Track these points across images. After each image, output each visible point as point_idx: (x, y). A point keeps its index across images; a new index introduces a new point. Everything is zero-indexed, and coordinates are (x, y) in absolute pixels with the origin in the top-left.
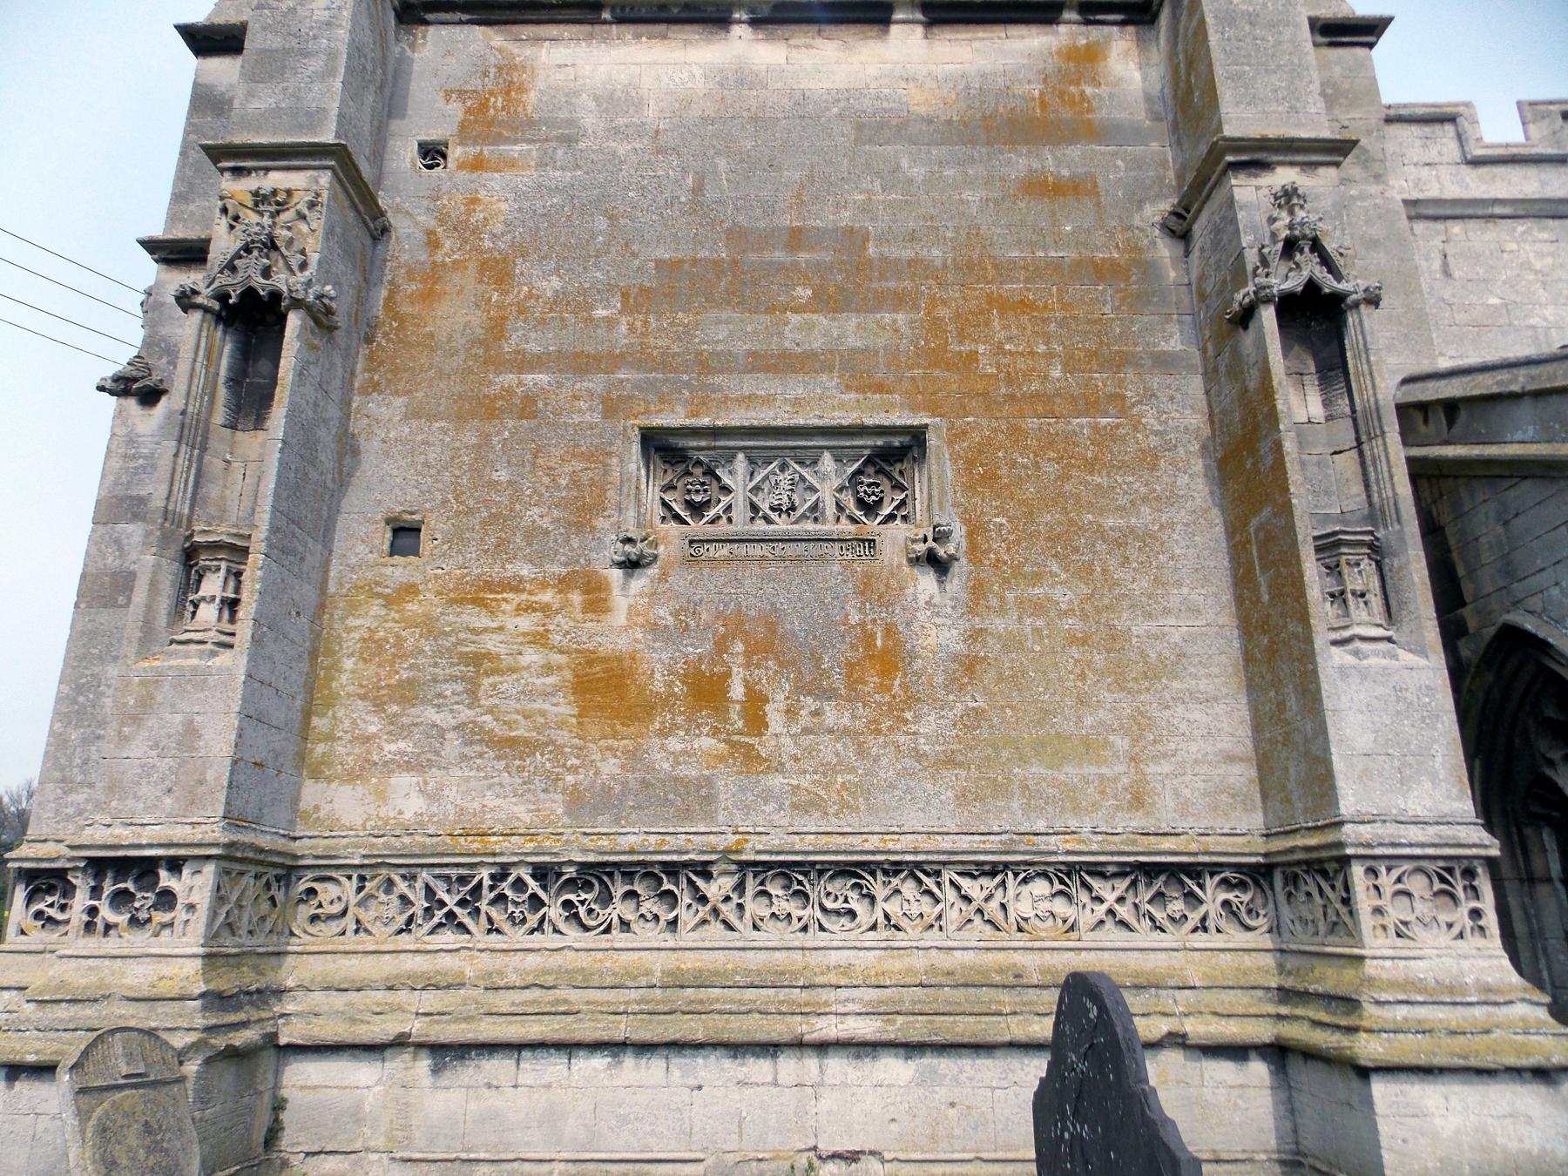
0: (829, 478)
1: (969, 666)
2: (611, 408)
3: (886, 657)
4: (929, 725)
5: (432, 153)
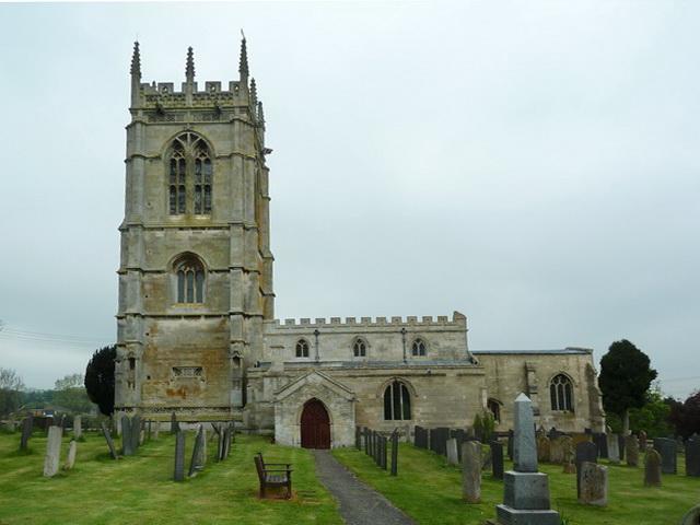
0: (192, 371)
1: (206, 390)
2: (170, 364)
3: (197, 389)
4: (201, 396)
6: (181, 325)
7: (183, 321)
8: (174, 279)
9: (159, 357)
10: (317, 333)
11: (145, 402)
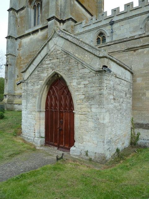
5: (18, 49)
6: (31, 39)
7: (32, 36)
8: (31, 11)
9: (22, 63)
10: (112, 23)
11: (16, 92)
